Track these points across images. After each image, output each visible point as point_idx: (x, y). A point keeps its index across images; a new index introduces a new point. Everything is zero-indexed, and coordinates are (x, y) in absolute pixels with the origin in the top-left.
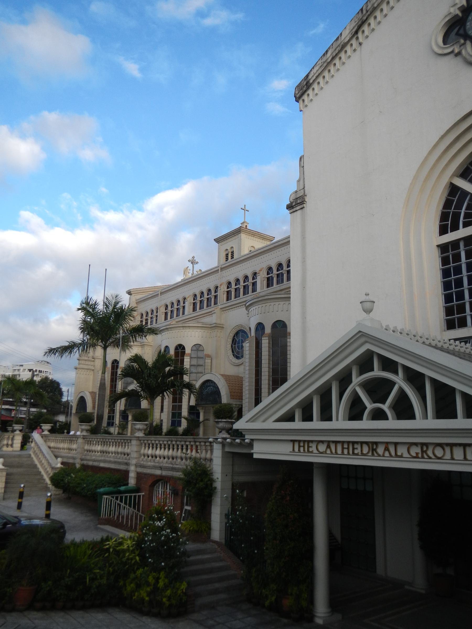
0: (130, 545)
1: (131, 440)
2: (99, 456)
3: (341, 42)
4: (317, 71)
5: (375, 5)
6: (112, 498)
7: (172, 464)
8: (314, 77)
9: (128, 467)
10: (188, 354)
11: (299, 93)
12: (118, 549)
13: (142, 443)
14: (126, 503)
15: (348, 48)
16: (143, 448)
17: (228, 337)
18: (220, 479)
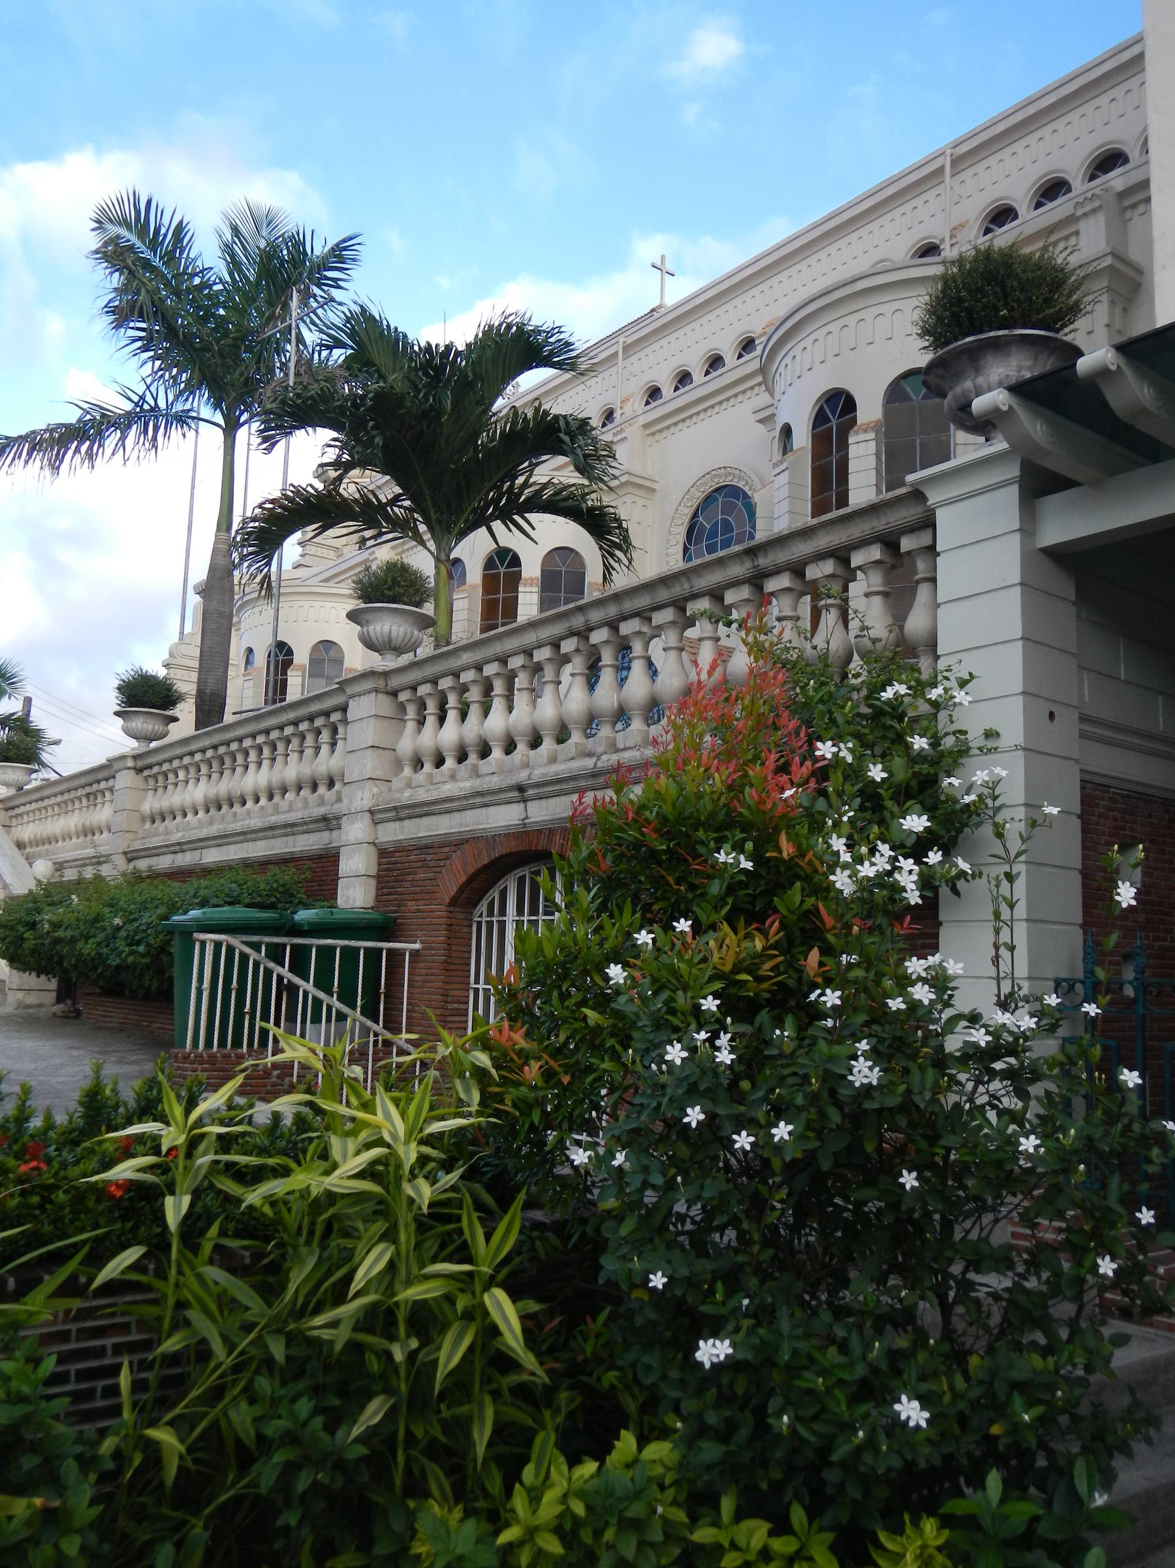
0: (409, 1154)
1: (344, 709)
2: (201, 824)
6: (247, 950)
7: (590, 755)
9: (335, 833)
10: (532, 579)
12: (254, 1197)
13: (402, 707)
14: (323, 983)
16: (411, 726)
17: (672, 521)
18: (1013, 731)
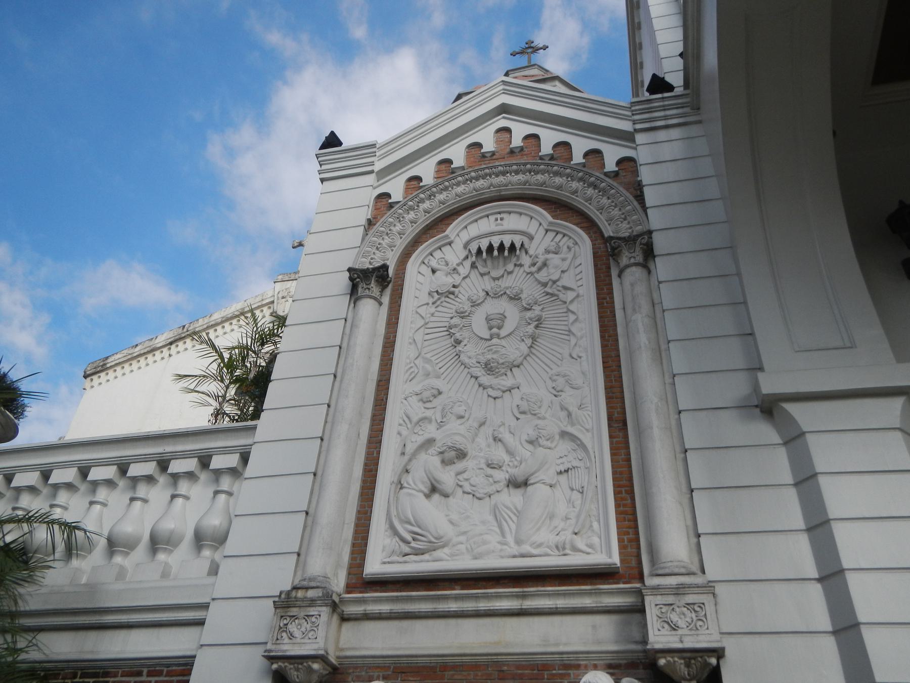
3: (153, 345)
4: (119, 358)
5: (197, 330)
8: (113, 364)
11: (90, 370)
15: (157, 353)
